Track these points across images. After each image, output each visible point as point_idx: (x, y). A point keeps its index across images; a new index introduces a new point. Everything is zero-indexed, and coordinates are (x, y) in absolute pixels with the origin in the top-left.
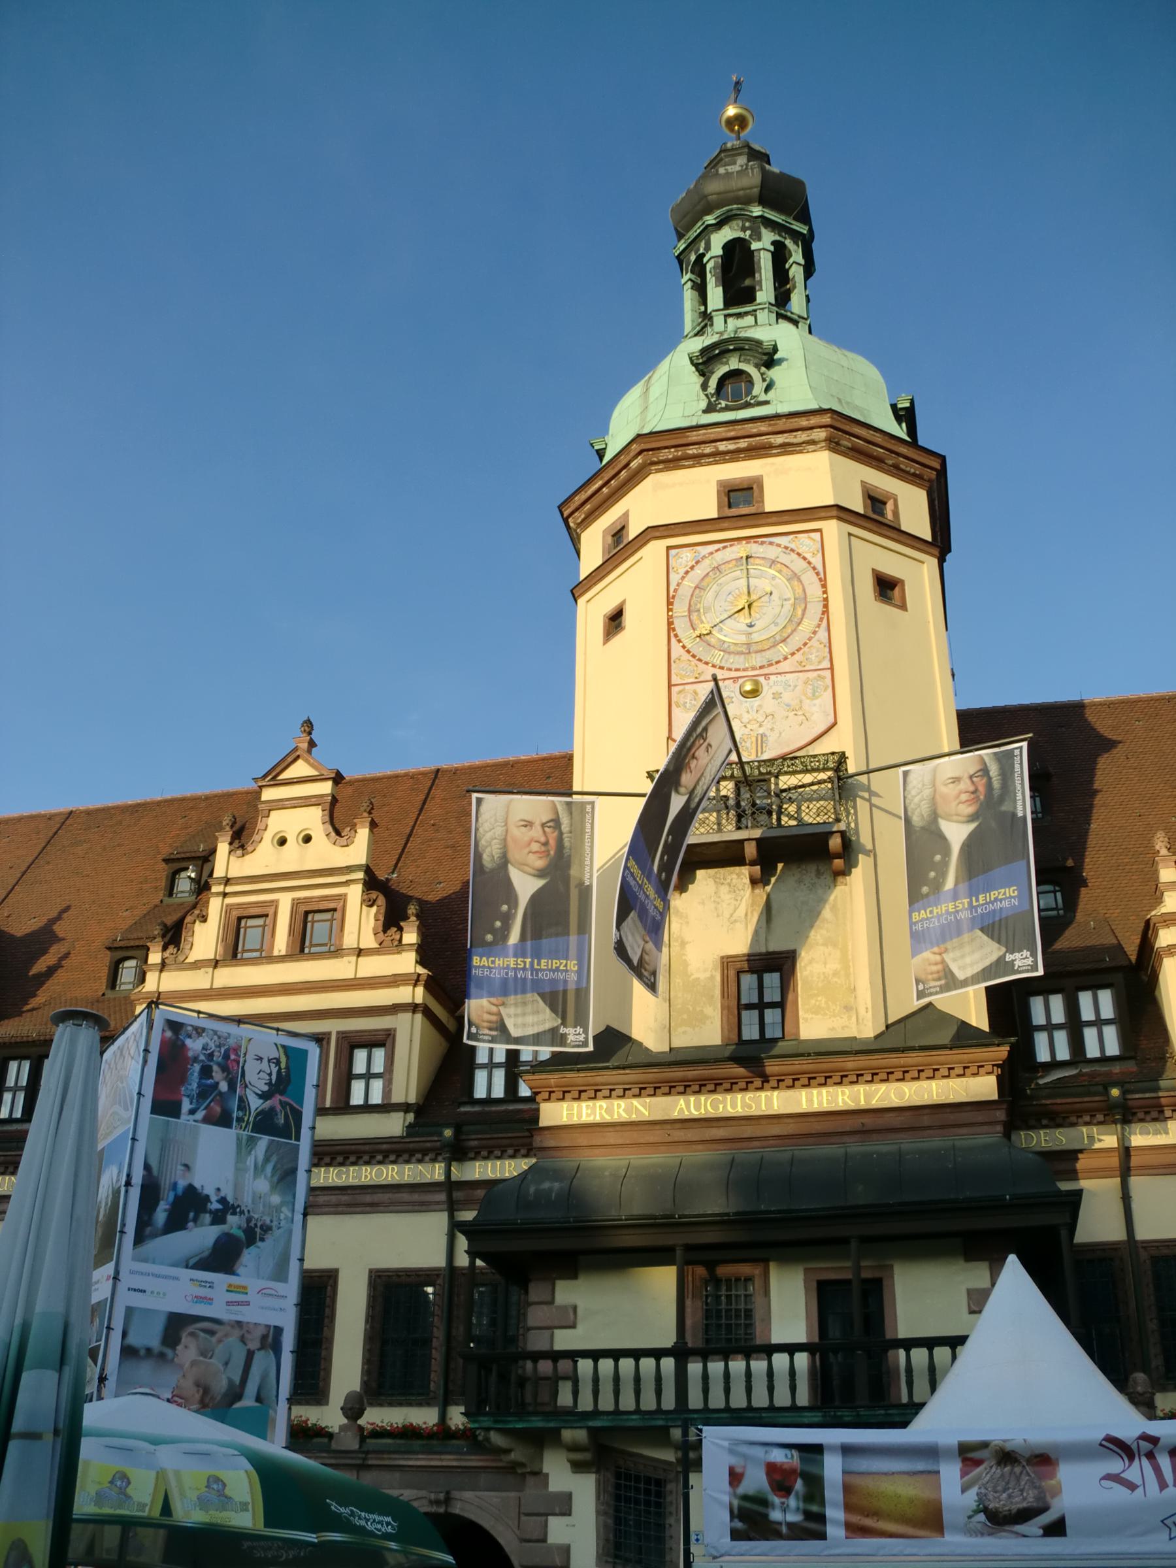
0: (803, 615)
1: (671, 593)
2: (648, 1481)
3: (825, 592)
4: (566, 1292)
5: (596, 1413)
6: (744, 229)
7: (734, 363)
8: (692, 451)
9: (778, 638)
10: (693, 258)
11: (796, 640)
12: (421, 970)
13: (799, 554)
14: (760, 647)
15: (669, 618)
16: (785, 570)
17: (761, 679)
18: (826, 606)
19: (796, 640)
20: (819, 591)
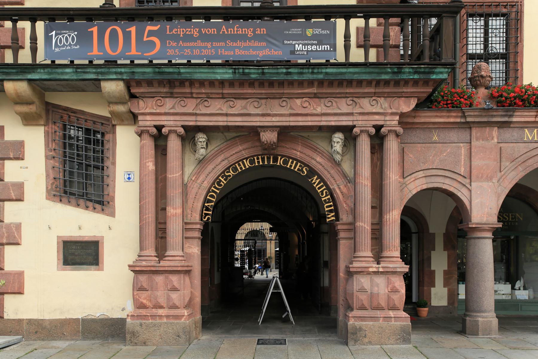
5: (33, 67)
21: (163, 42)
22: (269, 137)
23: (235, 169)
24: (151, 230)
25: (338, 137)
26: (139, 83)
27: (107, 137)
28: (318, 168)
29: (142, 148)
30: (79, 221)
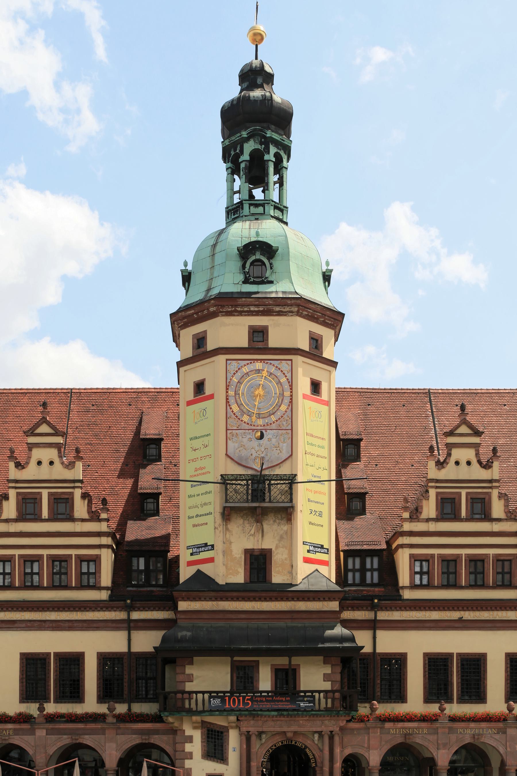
0: (282, 402)
1: (228, 384)
2: (218, 732)
3: (291, 392)
4: (189, 670)
6: (261, 144)
8: (239, 309)
9: (271, 412)
10: (233, 153)
11: (279, 414)
13: (282, 371)
14: (263, 416)
15: (227, 396)
16: (275, 378)
17: (264, 431)
18: (291, 399)
19: (279, 414)
20: (290, 391)
21: (252, 703)
22: (289, 735)
23: (275, 746)
25: (316, 736)
27: (225, 734)
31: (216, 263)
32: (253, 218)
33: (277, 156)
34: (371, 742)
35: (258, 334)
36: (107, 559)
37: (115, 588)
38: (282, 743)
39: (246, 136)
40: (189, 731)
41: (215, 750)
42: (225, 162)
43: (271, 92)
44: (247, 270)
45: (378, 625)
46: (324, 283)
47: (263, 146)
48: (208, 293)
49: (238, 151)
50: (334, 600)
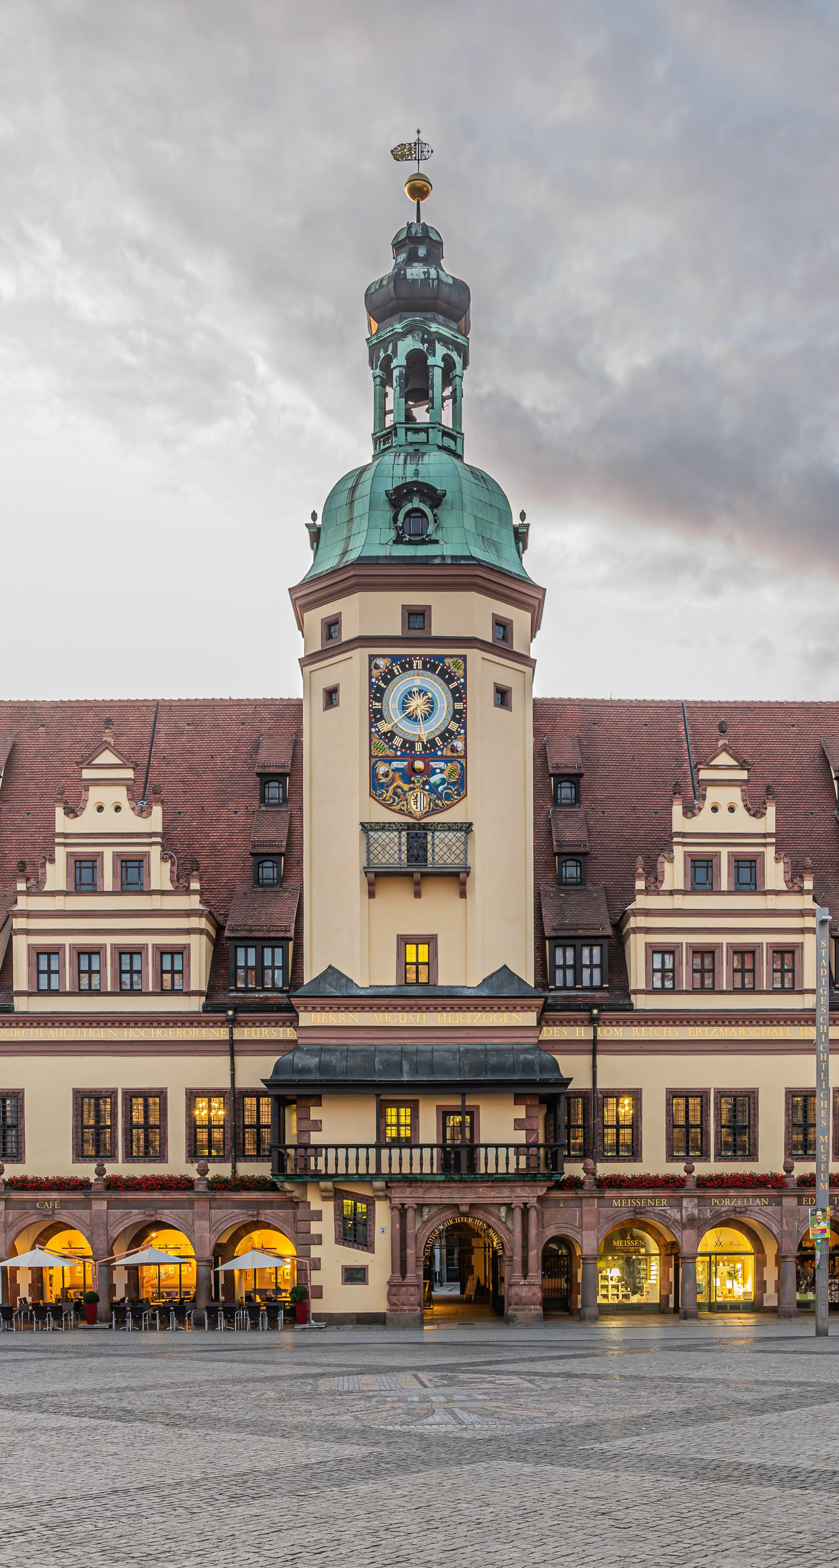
4: (315, 1113)
5: (337, 1175)
6: (423, 341)
7: (416, 503)
10: (382, 355)
12: (201, 907)
24: (398, 1262)
25: (503, 1210)
26: (393, 1182)
28: (492, 1224)
29: (392, 1217)
30: (356, 1257)
31: (356, 514)
32: (411, 449)
33: (446, 358)
34: (586, 1219)
35: (417, 617)
36: (199, 951)
37: (210, 993)
38: (454, 1221)
39: (401, 330)
40: (315, 1202)
41: (354, 1232)
42: (372, 369)
43: (439, 267)
44: (399, 524)
45: (599, 1047)
46: (517, 543)
47: (426, 345)
48: (343, 558)
49: (389, 352)
50: (529, 1008)
